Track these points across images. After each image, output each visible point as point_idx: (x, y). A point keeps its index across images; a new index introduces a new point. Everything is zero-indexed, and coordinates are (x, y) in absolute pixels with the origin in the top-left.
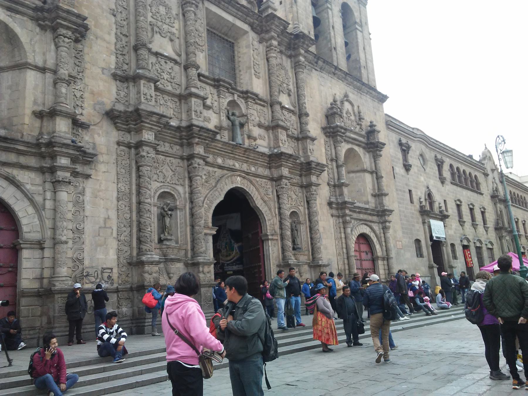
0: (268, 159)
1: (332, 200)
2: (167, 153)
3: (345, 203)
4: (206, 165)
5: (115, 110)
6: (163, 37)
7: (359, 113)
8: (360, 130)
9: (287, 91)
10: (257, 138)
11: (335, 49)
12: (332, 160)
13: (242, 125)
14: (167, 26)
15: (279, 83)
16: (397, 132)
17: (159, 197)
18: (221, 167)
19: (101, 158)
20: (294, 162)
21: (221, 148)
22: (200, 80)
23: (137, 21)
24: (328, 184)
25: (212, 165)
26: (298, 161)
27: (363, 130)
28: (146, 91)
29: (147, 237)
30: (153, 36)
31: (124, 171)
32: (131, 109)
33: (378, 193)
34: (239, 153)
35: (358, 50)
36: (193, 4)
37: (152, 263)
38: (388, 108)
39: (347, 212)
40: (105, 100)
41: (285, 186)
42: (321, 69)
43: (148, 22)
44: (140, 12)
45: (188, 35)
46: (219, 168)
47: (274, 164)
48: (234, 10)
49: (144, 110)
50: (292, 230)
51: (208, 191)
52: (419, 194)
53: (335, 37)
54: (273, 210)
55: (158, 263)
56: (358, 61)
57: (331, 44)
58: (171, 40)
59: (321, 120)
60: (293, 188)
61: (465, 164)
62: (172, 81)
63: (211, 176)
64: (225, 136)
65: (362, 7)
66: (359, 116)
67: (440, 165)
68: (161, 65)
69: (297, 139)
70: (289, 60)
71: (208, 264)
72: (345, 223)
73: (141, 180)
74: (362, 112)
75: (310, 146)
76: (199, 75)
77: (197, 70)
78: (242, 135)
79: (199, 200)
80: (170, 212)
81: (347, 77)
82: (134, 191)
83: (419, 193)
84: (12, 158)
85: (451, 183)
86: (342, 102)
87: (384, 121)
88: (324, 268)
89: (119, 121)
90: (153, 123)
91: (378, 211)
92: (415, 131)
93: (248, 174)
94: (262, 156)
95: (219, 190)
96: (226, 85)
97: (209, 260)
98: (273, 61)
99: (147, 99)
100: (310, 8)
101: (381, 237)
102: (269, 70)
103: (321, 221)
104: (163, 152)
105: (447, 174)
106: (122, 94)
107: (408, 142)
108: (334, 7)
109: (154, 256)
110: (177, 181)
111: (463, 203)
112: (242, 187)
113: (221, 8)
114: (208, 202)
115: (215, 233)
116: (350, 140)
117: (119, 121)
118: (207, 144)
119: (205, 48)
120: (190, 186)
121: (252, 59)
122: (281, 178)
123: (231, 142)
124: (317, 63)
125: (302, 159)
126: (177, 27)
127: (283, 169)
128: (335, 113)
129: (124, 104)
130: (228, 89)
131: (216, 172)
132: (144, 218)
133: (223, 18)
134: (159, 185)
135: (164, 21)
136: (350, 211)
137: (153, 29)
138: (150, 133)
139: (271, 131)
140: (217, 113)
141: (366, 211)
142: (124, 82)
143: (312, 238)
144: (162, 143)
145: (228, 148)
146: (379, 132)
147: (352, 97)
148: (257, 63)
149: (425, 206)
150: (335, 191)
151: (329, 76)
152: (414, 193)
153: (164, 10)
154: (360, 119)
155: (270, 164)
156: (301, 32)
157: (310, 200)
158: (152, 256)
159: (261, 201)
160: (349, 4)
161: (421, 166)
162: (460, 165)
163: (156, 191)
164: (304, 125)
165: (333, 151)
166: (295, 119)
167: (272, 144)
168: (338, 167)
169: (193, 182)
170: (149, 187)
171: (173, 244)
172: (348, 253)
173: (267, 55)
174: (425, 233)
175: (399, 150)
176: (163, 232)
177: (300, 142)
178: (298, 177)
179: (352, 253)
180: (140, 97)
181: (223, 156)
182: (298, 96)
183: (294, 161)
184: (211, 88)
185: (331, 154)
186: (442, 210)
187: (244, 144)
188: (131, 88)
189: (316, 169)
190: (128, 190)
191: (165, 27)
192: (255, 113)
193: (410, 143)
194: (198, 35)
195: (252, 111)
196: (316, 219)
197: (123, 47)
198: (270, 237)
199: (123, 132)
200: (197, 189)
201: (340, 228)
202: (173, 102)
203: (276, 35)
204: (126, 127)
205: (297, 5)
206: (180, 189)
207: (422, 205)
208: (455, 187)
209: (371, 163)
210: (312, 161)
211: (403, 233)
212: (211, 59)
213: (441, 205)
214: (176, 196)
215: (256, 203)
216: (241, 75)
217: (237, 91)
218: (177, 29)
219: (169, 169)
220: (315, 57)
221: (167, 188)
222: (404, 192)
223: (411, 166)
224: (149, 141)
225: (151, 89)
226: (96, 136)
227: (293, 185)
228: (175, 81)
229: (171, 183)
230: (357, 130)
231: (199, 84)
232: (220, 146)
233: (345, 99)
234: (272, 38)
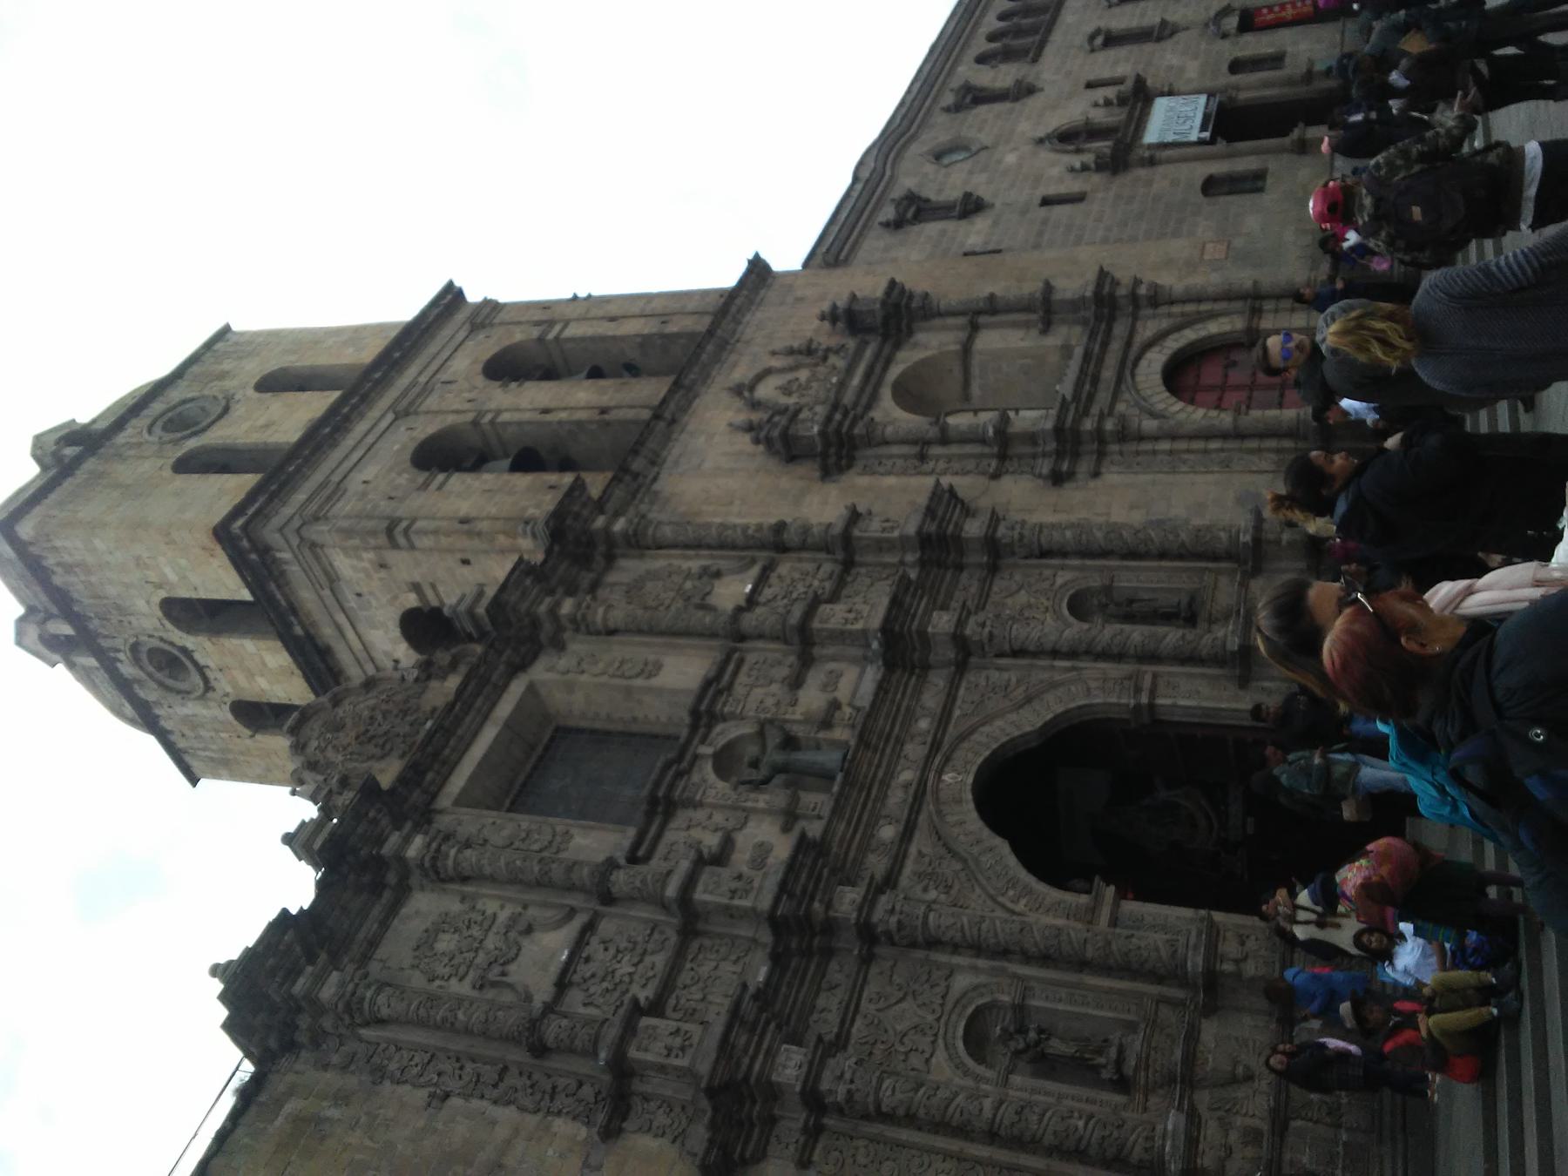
0: (899, 672)
1: (1045, 471)
2: (847, 1007)
3: (1058, 431)
4: (894, 887)
5: (704, 1159)
6: (517, 955)
7: (791, 352)
8: (842, 354)
9: (705, 579)
10: (830, 696)
11: (604, 411)
12: (922, 457)
13: (790, 743)
14: (491, 934)
15: (680, 604)
16: (861, 234)
17: (979, 1057)
18: (907, 834)
20: (916, 590)
21: (849, 823)
22: (647, 859)
23: (468, 1031)
24: (995, 476)
25: (899, 860)
26: (913, 574)
27: (843, 346)
28: (659, 1046)
29: (1103, 1138)
30: (510, 986)
31: (888, 1165)
32: (705, 1103)
33: (1041, 313)
34: (870, 764)
35: (614, 338)
36: (438, 850)
37: (1192, 1142)
38: (788, 257)
39: (1088, 425)
41: (987, 630)
42: (653, 463)
43: (475, 994)
44: (444, 1020)
45: (520, 876)
46: (910, 840)
47: (916, 656)
48: (468, 719)
49: (714, 1069)
50: (1129, 618)
51: (978, 890)
52: (1056, 170)
53: (572, 408)
54: (1057, 677)
55: (1193, 1118)
56: (645, 341)
57: (591, 422)
58: (529, 930)
59: (801, 478)
60: (994, 598)
61: (983, 15)
62: (639, 950)
63: (930, 870)
64: (817, 801)
65: (502, 316)
66: (800, 352)
67: (975, 97)
68: (593, 976)
69: (848, 565)
70: (623, 563)
71: (1213, 935)
72: (1123, 435)
73: (922, 1112)
74: (788, 344)
75: (873, 528)
76: (633, 859)
77: (618, 867)
78: (818, 747)
79: (1003, 930)
80: (1032, 1035)
81: (687, 382)
82: (954, 1145)
83: (1055, 171)
85: (1035, 60)
86: (755, 405)
87: (824, 272)
88: (1266, 526)
89: (739, 1149)
90: (753, 1045)
91: (1096, 318)
92: (865, 174)
93: (935, 746)
94: (886, 692)
95: (975, 850)
96: (668, 778)
97: (1199, 934)
98: (618, 616)
99: (683, 1049)
100: (487, 479)
101: (1183, 314)
102: (640, 632)
103: (1108, 514)
104: (843, 1022)
105: (1003, 76)
106: (661, 1119)
107: (893, 200)
108: (493, 405)
109: (1170, 1127)
110: (937, 990)
111: (1102, 24)
112: (974, 769)
113: (460, 758)
114: (1011, 893)
115: (1112, 888)
116: (869, 389)
117: (739, 1149)
118: (833, 872)
119: (560, 824)
120: (956, 948)
121: (604, 679)
122: (959, 640)
123: (836, 788)
124: (636, 476)
125: (910, 558)
126: (496, 905)
127: (934, 627)
128: (785, 436)
129: (690, 1121)
130: (680, 775)
131: (920, 852)
132: (1041, 1131)
133: (486, 757)
134: (941, 1055)
135: (476, 945)
136: (1086, 413)
137: (494, 984)
138: (781, 1059)
139: (816, 651)
140: (746, 818)
141: (1094, 358)
142: (629, 1108)
143: (1163, 555)
144: (815, 1016)
145: (852, 802)
146: (853, 297)
147: (741, 372)
148: (617, 664)
149: (1098, 157)
150: (1020, 457)
151: (676, 440)
152: (1052, 190)
153: (446, 937)
154: (809, 350)
155: (913, 667)
156: (547, 523)
157: (1040, 545)
158: (1170, 1134)
159: (1026, 713)
160: (488, 355)
161: (970, 162)
162: (984, 30)
163: (959, 1066)
164: (809, 540)
165: (895, 450)
166: (788, 565)
167: (856, 652)
168: (945, 439)
169: (944, 939)
170: (943, 1094)
171: (1136, 1044)
172: (1225, 436)
173: (598, 633)
174: (1185, 159)
175: (916, 228)
176: (1096, 1069)
177: (857, 558)
178: (965, 575)
179: (1225, 419)
180: (676, 1068)
181: (873, 824)
182: (722, 546)
183: (912, 589)
184: (673, 825)
185: (905, 457)
186: (1118, 97)
187: (847, 743)
188: (647, 1088)
189: (943, 519)
190: (948, 1165)
191: (490, 943)
192: (758, 693)
193: (897, 192)
194: (523, 840)
195: (752, 705)
196: (1099, 535)
197: (532, 1086)
198: (1144, 700)
199: (773, 1140)
200: (966, 927)
201: (1138, 453)
202: (701, 956)
203: (548, 600)
204: (757, 1131)
205: (475, 519)
206: (961, 982)
207: (1093, 166)
208: (1049, 50)
209: (945, 328)
210: (919, 532)
211: (1176, 234)
212: (592, 811)
213: (1101, 101)
214: (981, 1001)
215: (1028, 729)
216: (646, 716)
217: (689, 741)
218: (502, 907)
219: (896, 1007)
220: (620, 481)
221: (955, 1027)
222: (1045, 222)
223: (968, 195)
224: (805, 1069)
225: (655, 1028)
227: (988, 595)
228: (640, 939)
229: (939, 1009)
230: (838, 362)
231: (657, 864)
232: (842, 827)
233: (746, 394)
234: (553, 612)
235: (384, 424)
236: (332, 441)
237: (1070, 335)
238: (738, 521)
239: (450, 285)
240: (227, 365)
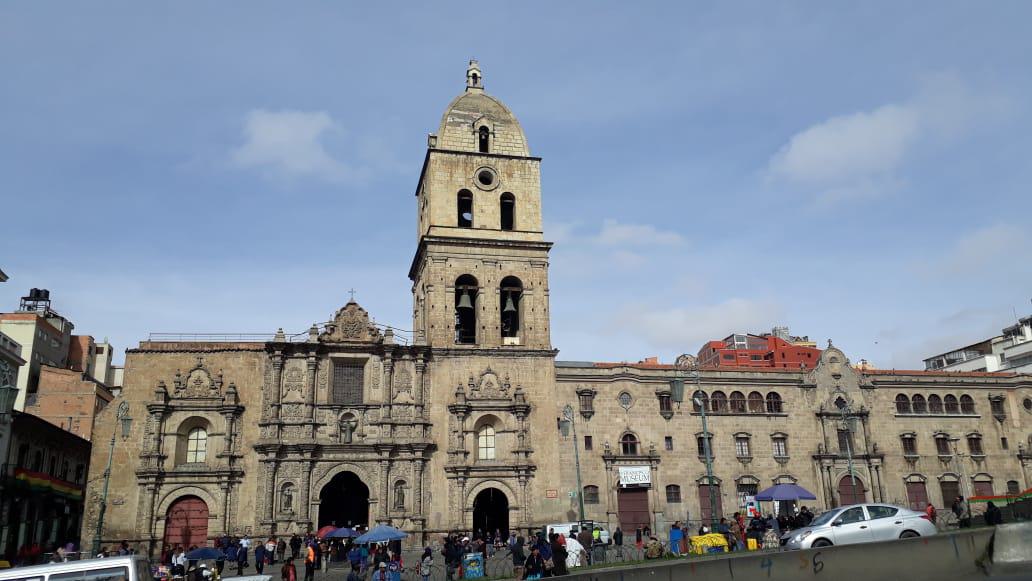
11: (484, 328)
84: (206, 479)
211: (562, 482)
235: (477, 257)
236: (468, 245)
239: (552, 244)
240: (517, 174)
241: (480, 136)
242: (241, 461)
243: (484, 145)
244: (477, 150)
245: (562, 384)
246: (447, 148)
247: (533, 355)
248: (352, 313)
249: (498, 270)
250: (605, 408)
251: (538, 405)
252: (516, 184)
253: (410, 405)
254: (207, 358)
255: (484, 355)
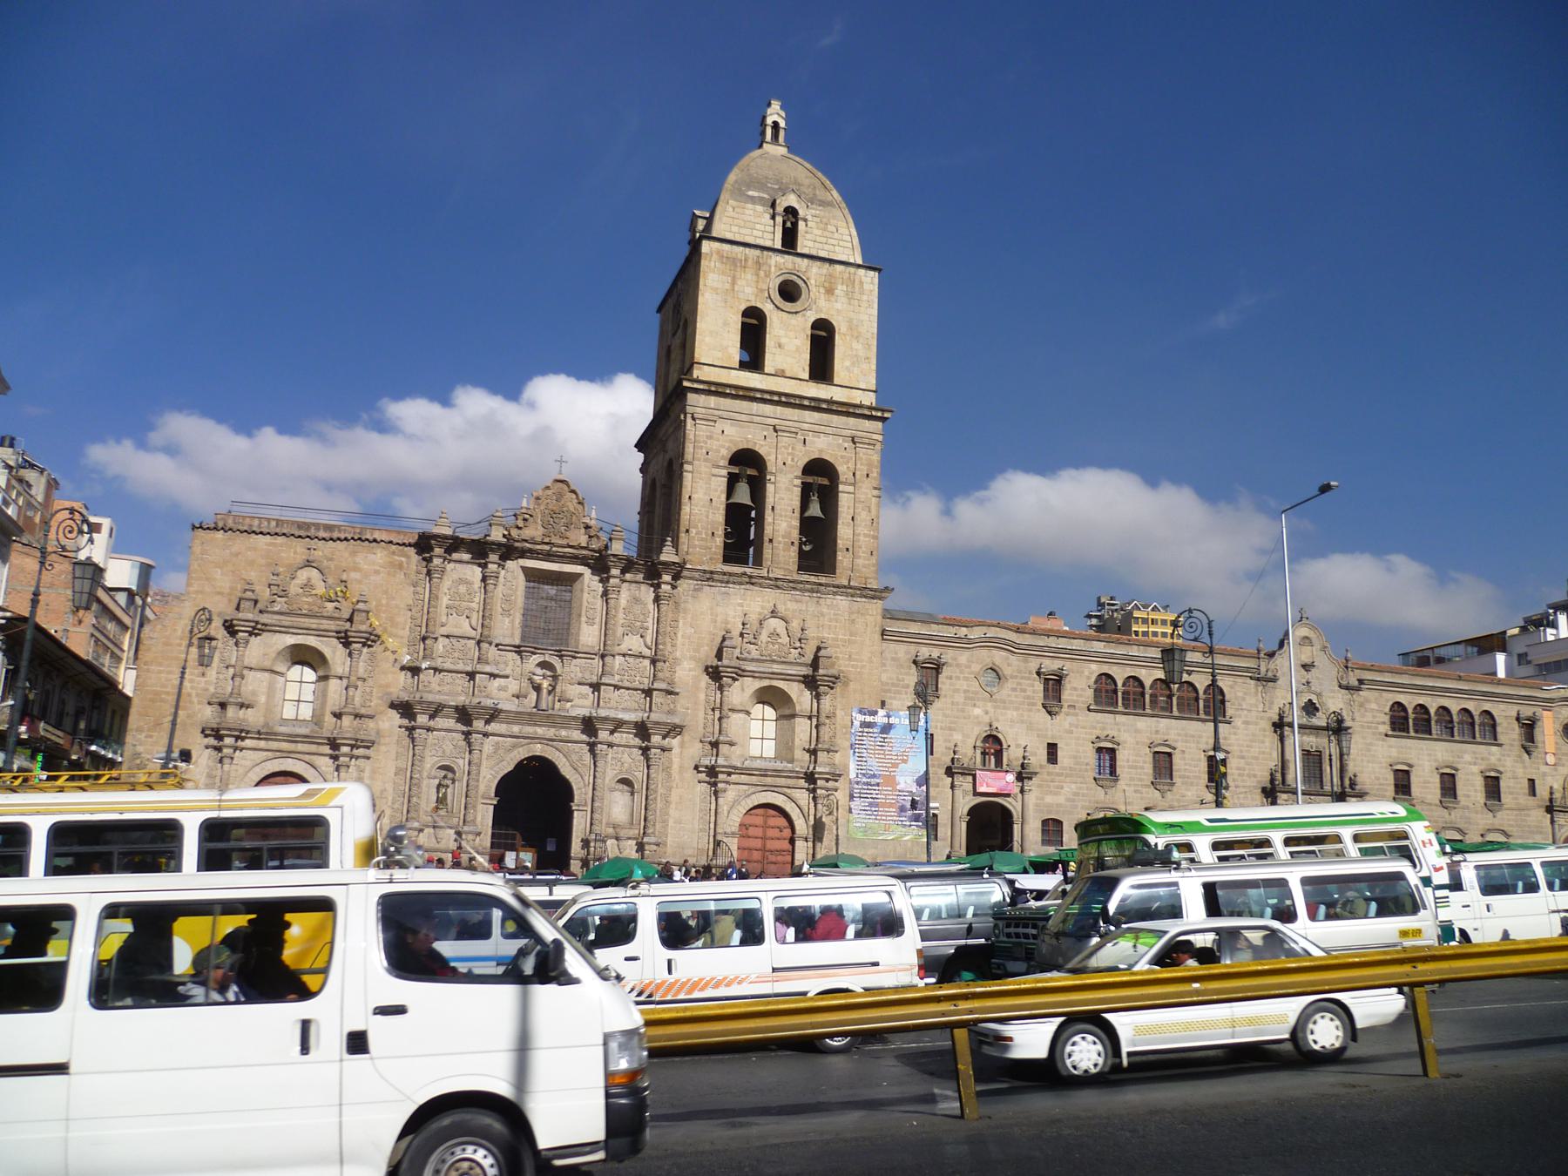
11: (771, 541)
12: (713, 710)
19: (382, 741)
40: (392, 690)
84: (313, 748)
126: (476, 603)
134: (437, 759)
191: (465, 604)
206: (461, 762)
226: (380, 723)
237: (802, 760)
238: (679, 635)
240: (840, 289)
241: (784, 222)
242: (371, 724)
243: (790, 239)
244: (778, 245)
245: (892, 646)
246: (729, 236)
247: (847, 595)
248: (559, 496)
249: (800, 446)
250: (957, 691)
251: (852, 677)
252: (838, 306)
253: (644, 657)
254: (323, 550)
255: (769, 587)
